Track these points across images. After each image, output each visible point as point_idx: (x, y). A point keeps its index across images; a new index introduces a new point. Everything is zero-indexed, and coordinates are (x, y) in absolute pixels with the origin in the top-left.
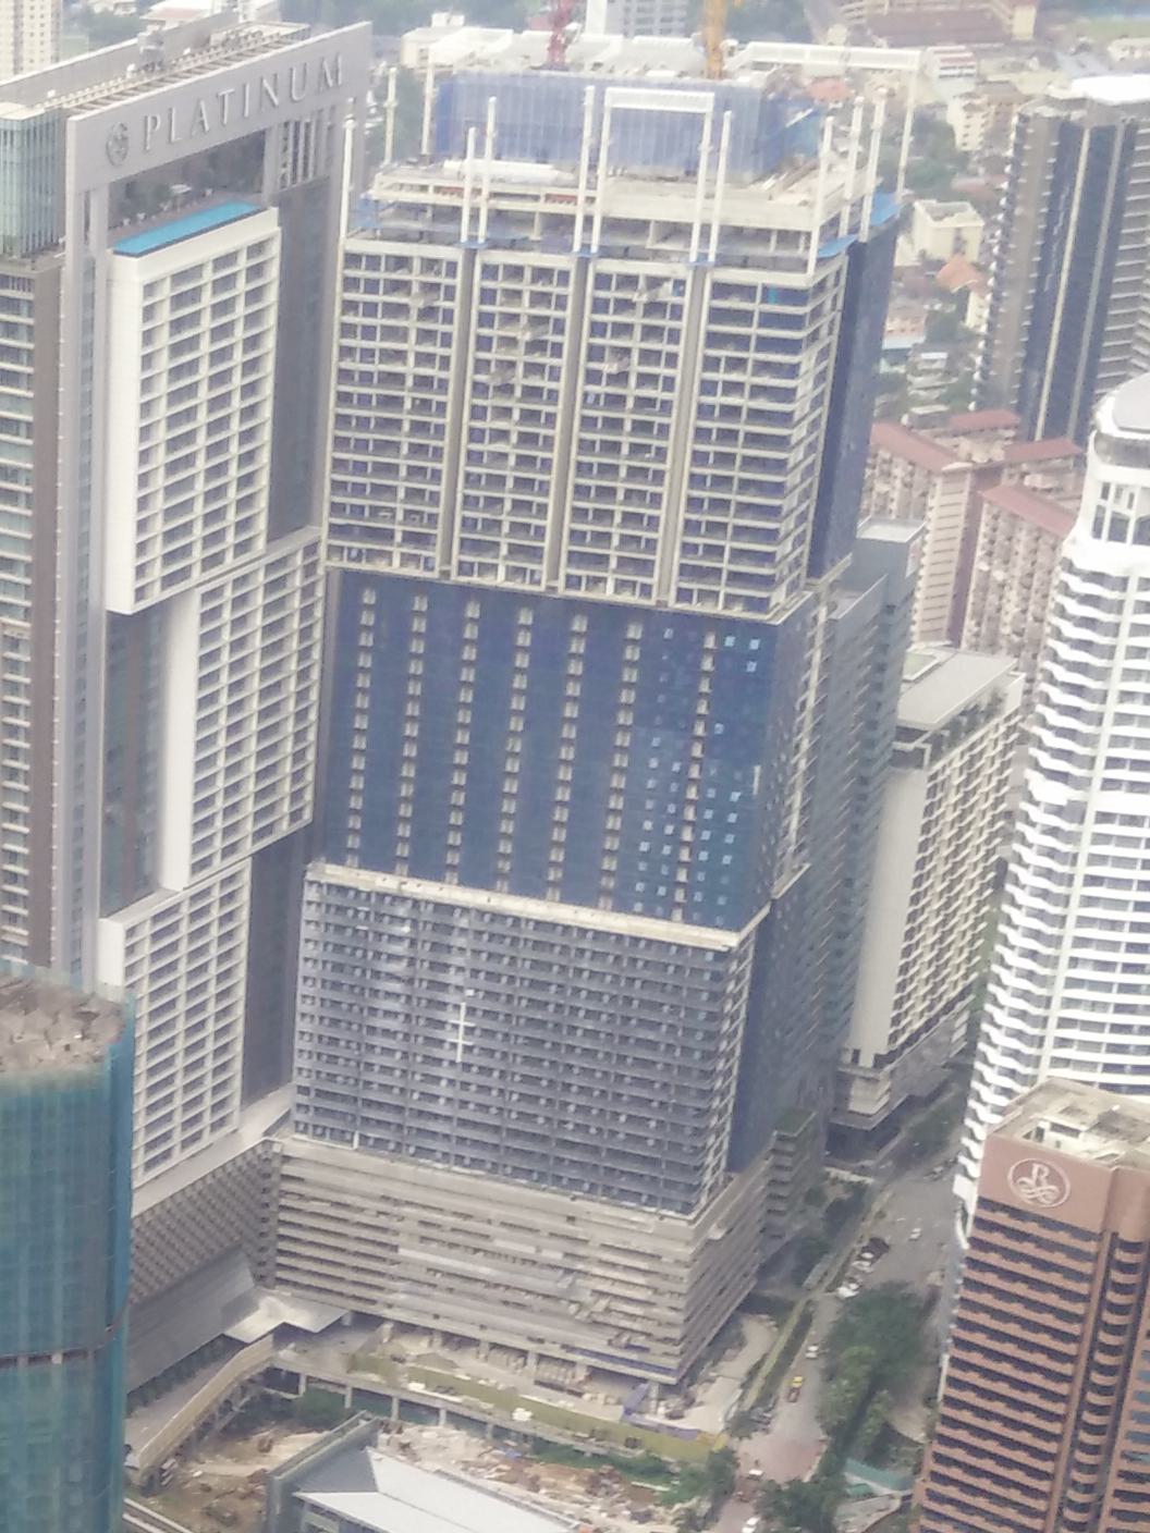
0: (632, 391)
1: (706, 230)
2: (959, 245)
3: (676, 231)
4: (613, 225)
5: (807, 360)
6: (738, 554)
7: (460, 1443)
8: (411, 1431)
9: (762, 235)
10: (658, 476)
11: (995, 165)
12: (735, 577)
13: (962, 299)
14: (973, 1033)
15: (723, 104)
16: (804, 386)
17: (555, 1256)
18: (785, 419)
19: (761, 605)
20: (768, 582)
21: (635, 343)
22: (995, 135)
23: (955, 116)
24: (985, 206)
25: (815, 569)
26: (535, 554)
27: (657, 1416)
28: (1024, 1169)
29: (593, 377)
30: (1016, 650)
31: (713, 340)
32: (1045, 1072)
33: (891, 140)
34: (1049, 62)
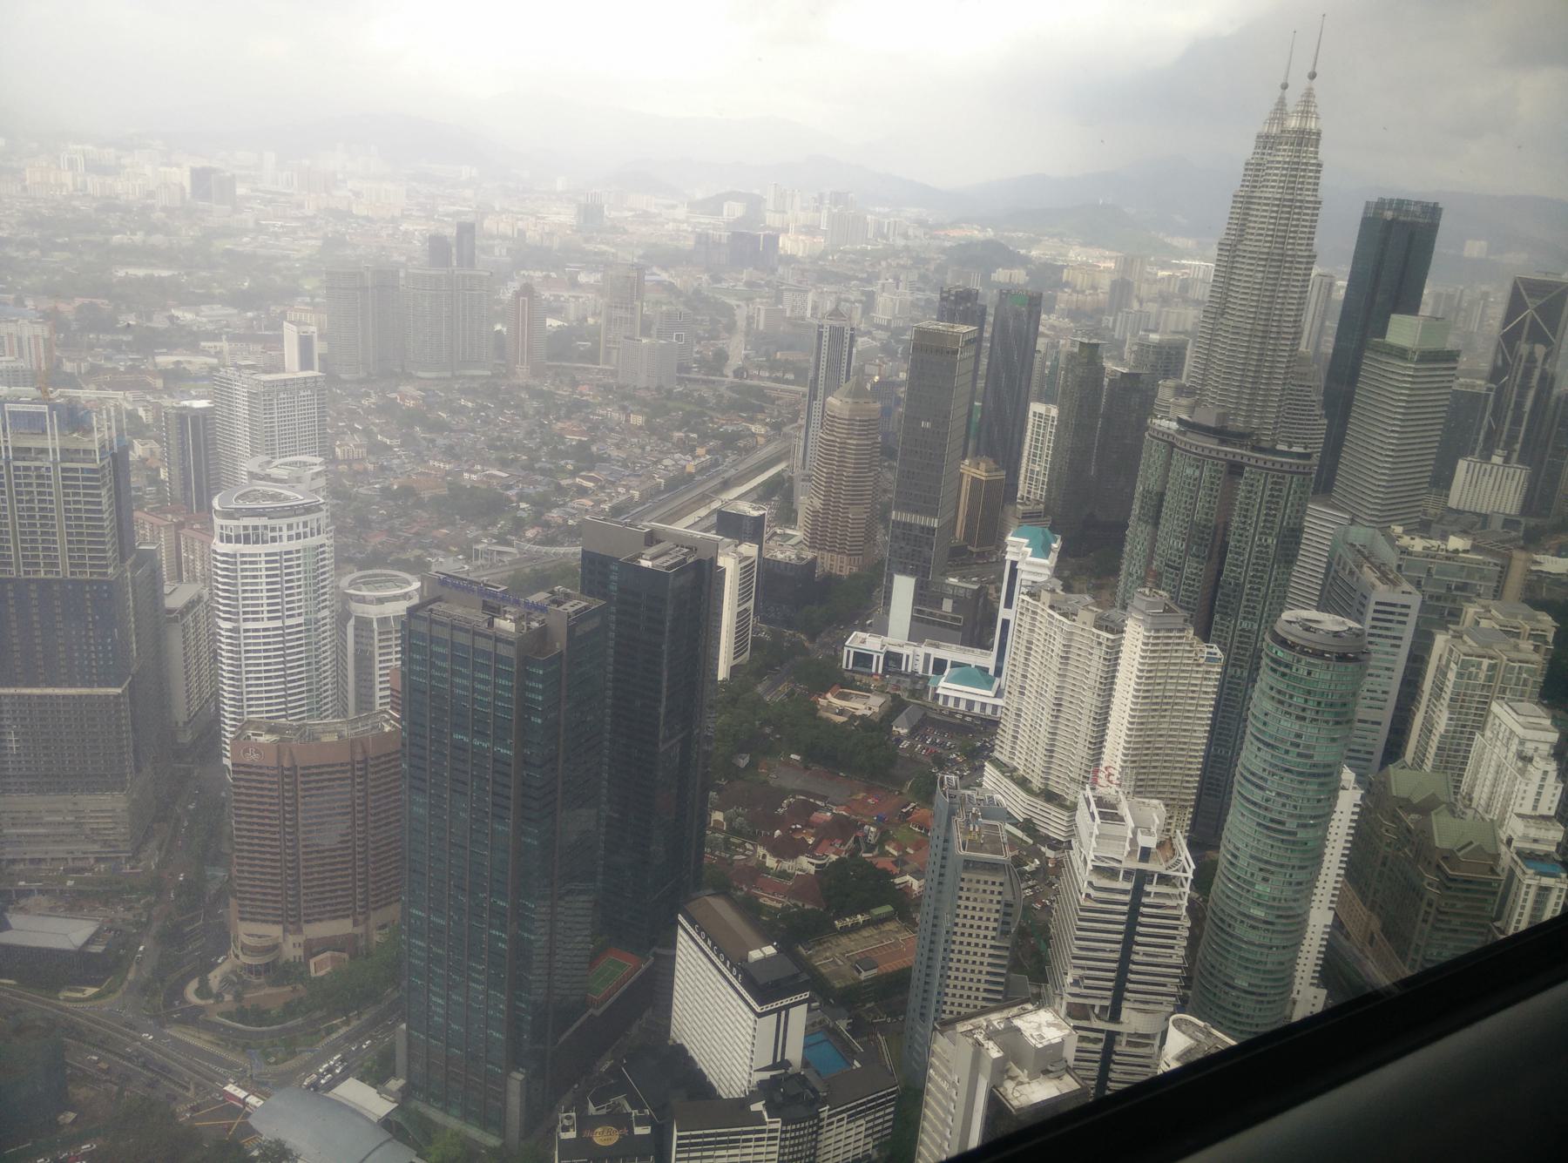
0: (36, 505)
1: (54, 451)
2: (152, 452)
3: (44, 451)
4: (15, 449)
5: (103, 492)
6: (91, 558)
7: (44, 901)
8: (23, 902)
9: (77, 451)
10: (54, 534)
11: (160, 429)
12: (92, 566)
13: (157, 470)
14: (218, 709)
15: (53, 407)
16: (104, 500)
17: (70, 819)
18: (100, 511)
19: (105, 574)
20: (107, 566)
21: (34, 489)
22: (157, 419)
23: (141, 412)
24: (159, 440)
25: (123, 559)
26: (10, 564)
27: (127, 869)
28: (246, 751)
29: (19, 501)
30: (204, 581)
31: (65, 487)
32: (246, 717)
33: (119, 421)
34: (171, 396)
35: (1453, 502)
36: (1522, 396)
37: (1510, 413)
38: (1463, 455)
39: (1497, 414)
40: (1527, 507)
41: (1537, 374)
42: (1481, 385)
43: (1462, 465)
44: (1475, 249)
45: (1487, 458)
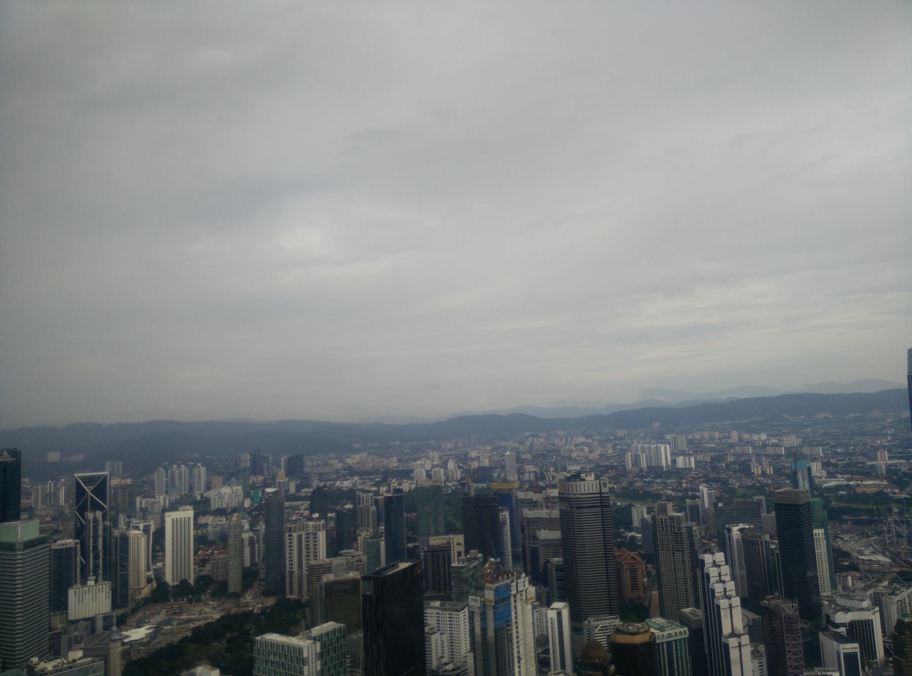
35: (71, 617)
36: (95, 542)
37: (91, 554)
38: (70, 585)
39: (84, 554)
40: (115, 605)
41: (101, 528)
42: (70, 542)
43: (71, 592)
44: (54, 457)
45: (84, 583)
